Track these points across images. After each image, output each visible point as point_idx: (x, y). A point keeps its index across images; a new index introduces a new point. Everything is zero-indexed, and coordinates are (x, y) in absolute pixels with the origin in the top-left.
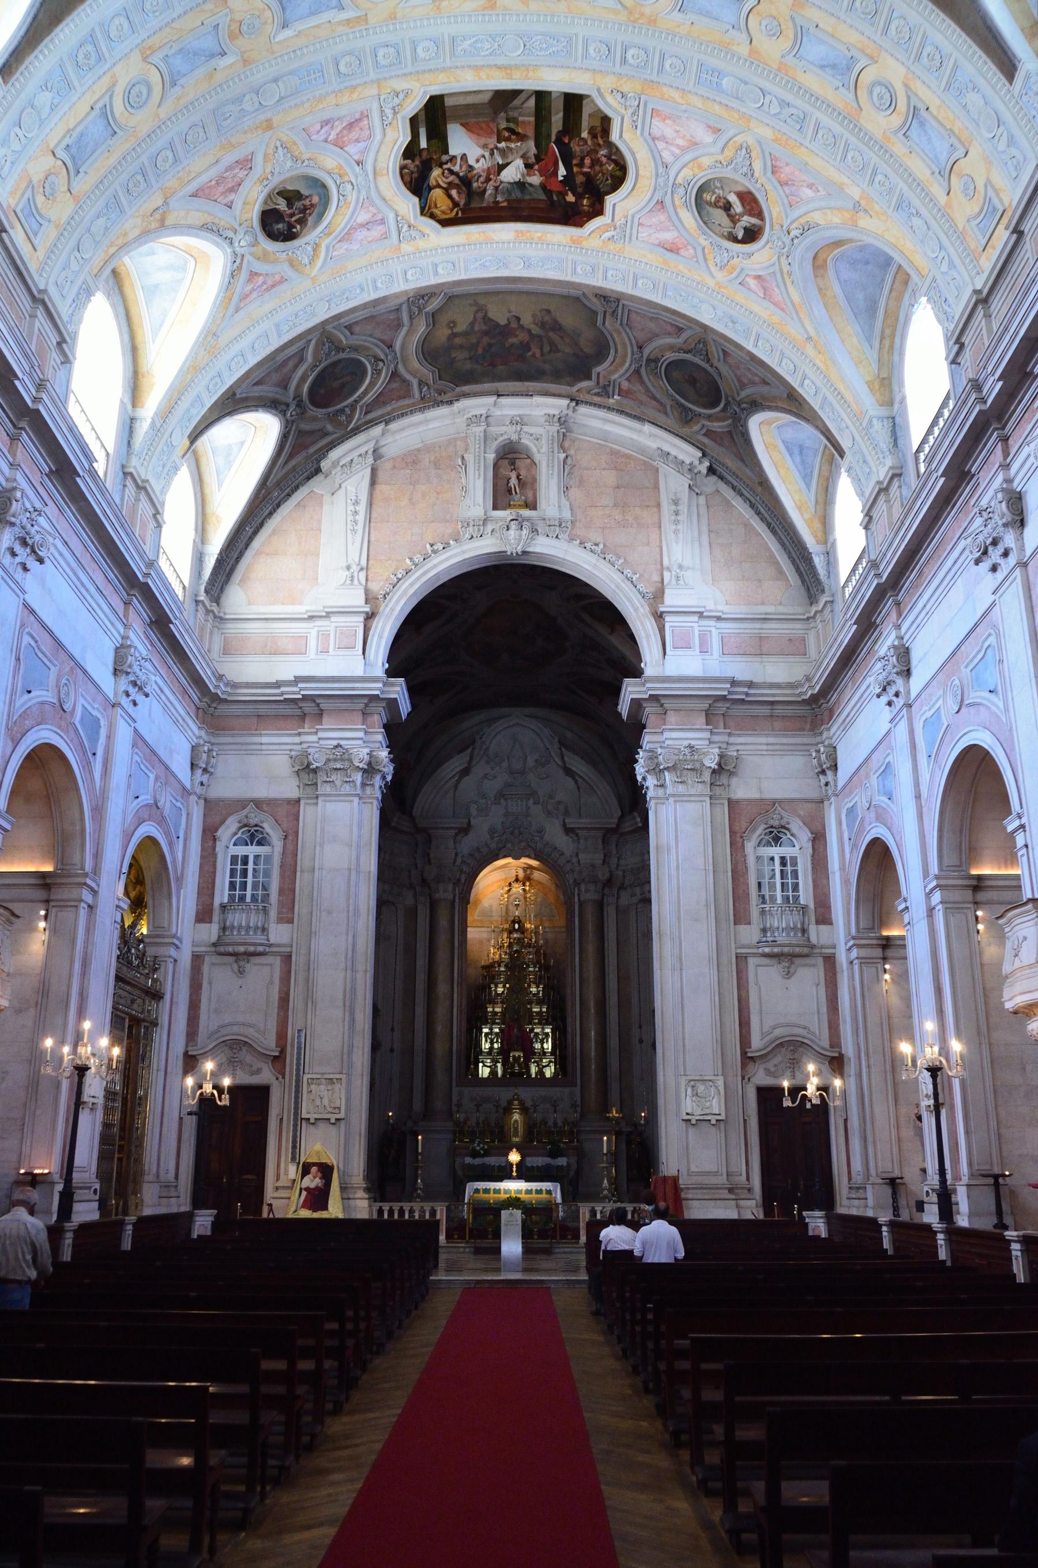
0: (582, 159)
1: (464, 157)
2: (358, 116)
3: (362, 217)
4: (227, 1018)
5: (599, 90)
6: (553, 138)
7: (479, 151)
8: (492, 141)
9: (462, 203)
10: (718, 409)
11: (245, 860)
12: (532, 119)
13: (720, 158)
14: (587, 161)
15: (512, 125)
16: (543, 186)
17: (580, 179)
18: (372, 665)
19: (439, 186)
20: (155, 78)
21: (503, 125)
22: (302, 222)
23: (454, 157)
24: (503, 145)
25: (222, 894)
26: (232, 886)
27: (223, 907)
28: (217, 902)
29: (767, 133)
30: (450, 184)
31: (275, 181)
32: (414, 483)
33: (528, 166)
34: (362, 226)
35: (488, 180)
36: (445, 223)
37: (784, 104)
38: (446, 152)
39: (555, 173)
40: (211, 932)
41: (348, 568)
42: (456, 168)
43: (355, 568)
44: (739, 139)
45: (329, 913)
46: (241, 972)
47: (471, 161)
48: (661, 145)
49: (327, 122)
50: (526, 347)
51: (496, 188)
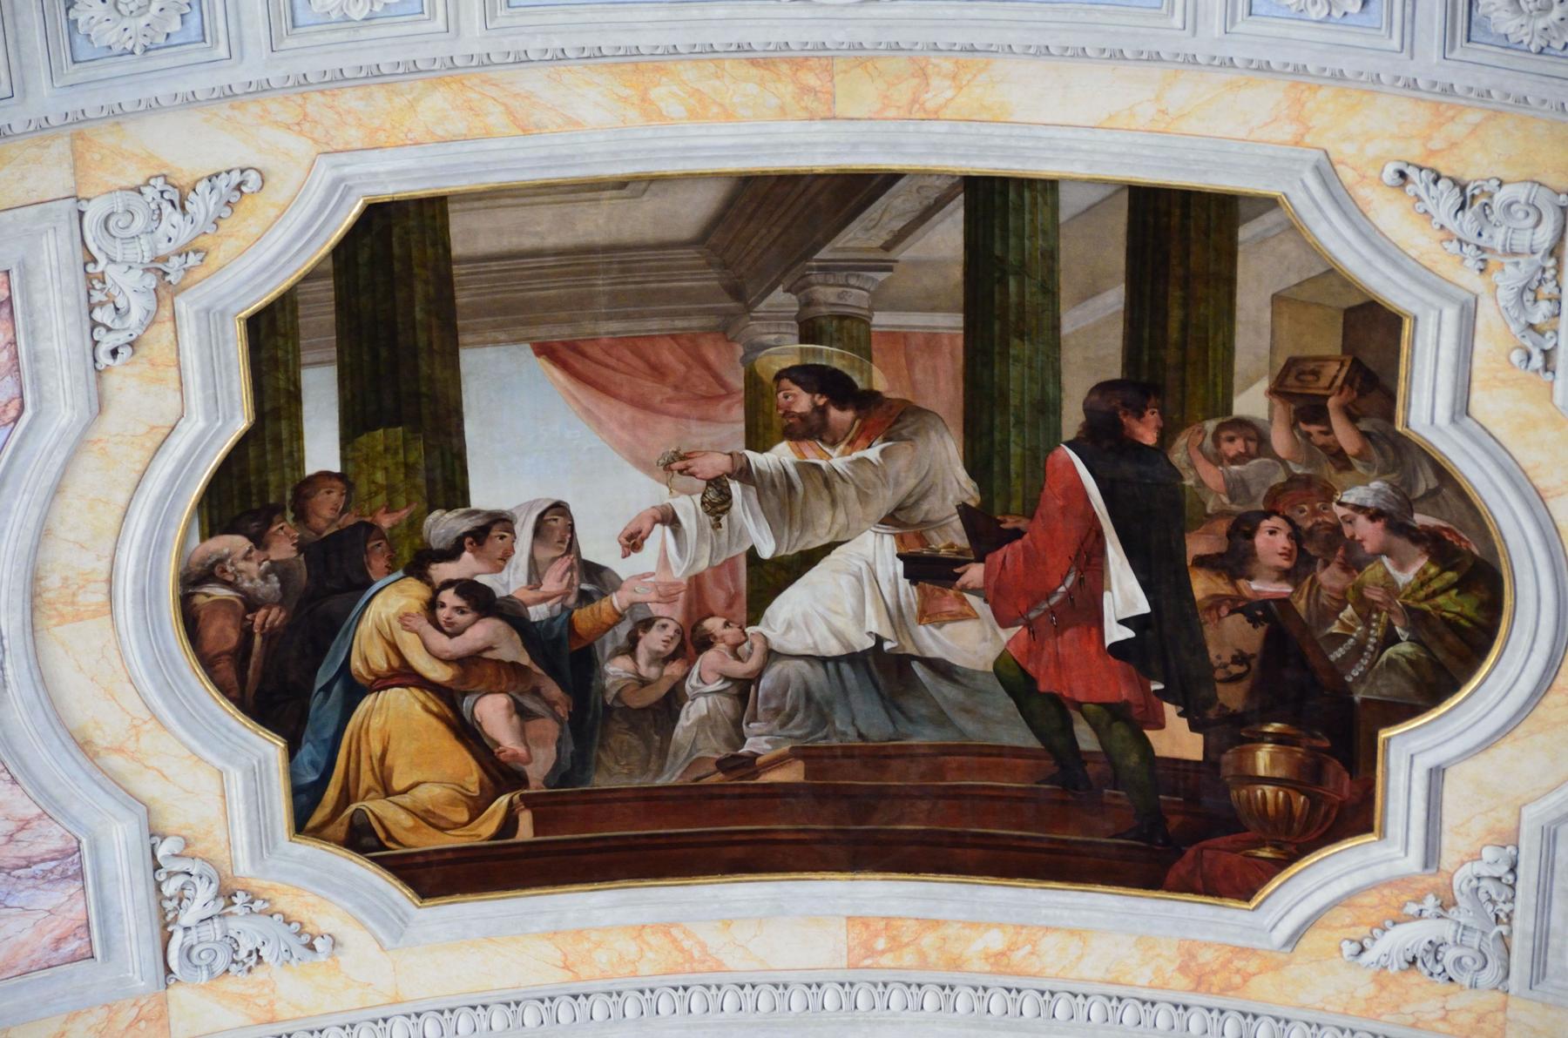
0: (1243, 529)
1: (555, 521)
5: (1326, 172)
6: (1072, 419)
7: (645, 491)
8: (719, 438)
9: (539, 767)
12: (951, 322)
14: (1271, 542)
15: (831, 356)
16: (1014, 677)
19: (404, 675)
24: (781, 456)
30: (469, 663)
33: (927, 570)
35: (693, 642)
39: (1086, 607)
42: (510, 581)
47: (598, 546)
51: (742, 689)
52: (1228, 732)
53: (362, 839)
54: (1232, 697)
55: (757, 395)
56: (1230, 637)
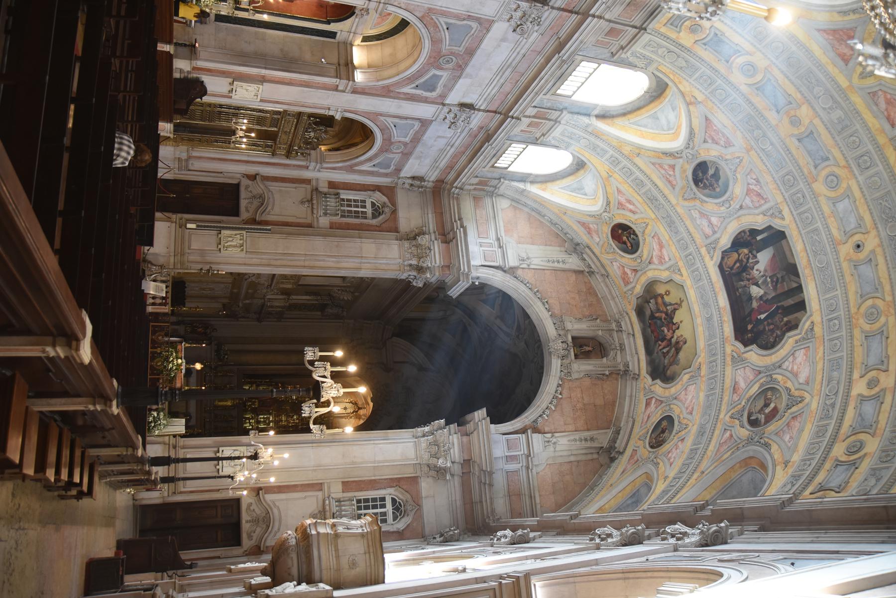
0: (772, 324)
1: (758, 262)
2: (765, 196)
3: (714, 220)
4: (277, 196)
8: (769, 273)
9: (733, 271)
10: (650, 449)
11: (365, 207)
13: (793, 390)
14: (772, 327)
17: (761, 327)
18: (477, 270)
19: (739, 255)
20: (759, 77)
21: (779, 276)
22: (705, 187)
23: (755, 257)
24: (769, 280)
25: (345, 195)
26: (349, 200)
27: (338, 194)
28: (341, 191)
29: (814, 405)
30: (742, 260)
31: (722, 164)
32: (579, 292)
33: (761, 297)
34: (710, 222)
35: (748, 280)
36: (721, 267)
37: (833, 405)
38: (758, 252)
40: (324, 188)
41: (528, 258)
42: (751, 261)
43: (528, 262)
44: (806, 395)
45: (337, 246)
46: (302, 202)
47: (756, 267)
48: (791, 359)
49: (757, 181)
50: (663, 340)
51: (745, 286)
52: (751, 331)
53: (723, 258)
54: (755, 330)
55: (775, 275)
56: (761, 327)
